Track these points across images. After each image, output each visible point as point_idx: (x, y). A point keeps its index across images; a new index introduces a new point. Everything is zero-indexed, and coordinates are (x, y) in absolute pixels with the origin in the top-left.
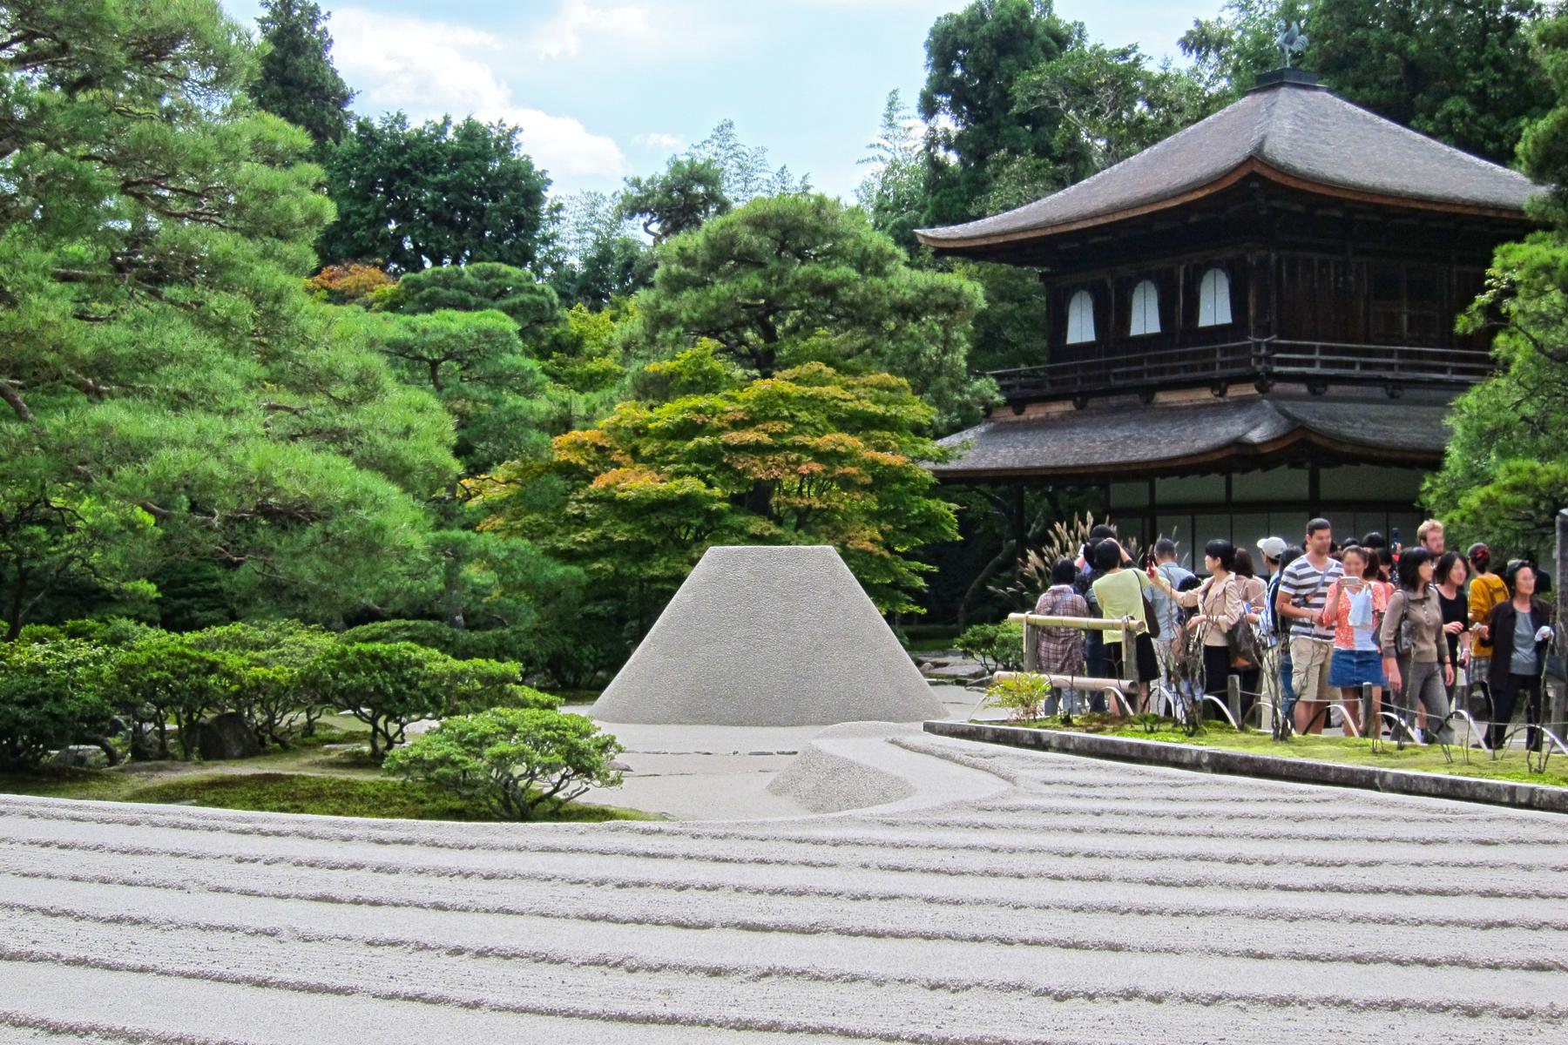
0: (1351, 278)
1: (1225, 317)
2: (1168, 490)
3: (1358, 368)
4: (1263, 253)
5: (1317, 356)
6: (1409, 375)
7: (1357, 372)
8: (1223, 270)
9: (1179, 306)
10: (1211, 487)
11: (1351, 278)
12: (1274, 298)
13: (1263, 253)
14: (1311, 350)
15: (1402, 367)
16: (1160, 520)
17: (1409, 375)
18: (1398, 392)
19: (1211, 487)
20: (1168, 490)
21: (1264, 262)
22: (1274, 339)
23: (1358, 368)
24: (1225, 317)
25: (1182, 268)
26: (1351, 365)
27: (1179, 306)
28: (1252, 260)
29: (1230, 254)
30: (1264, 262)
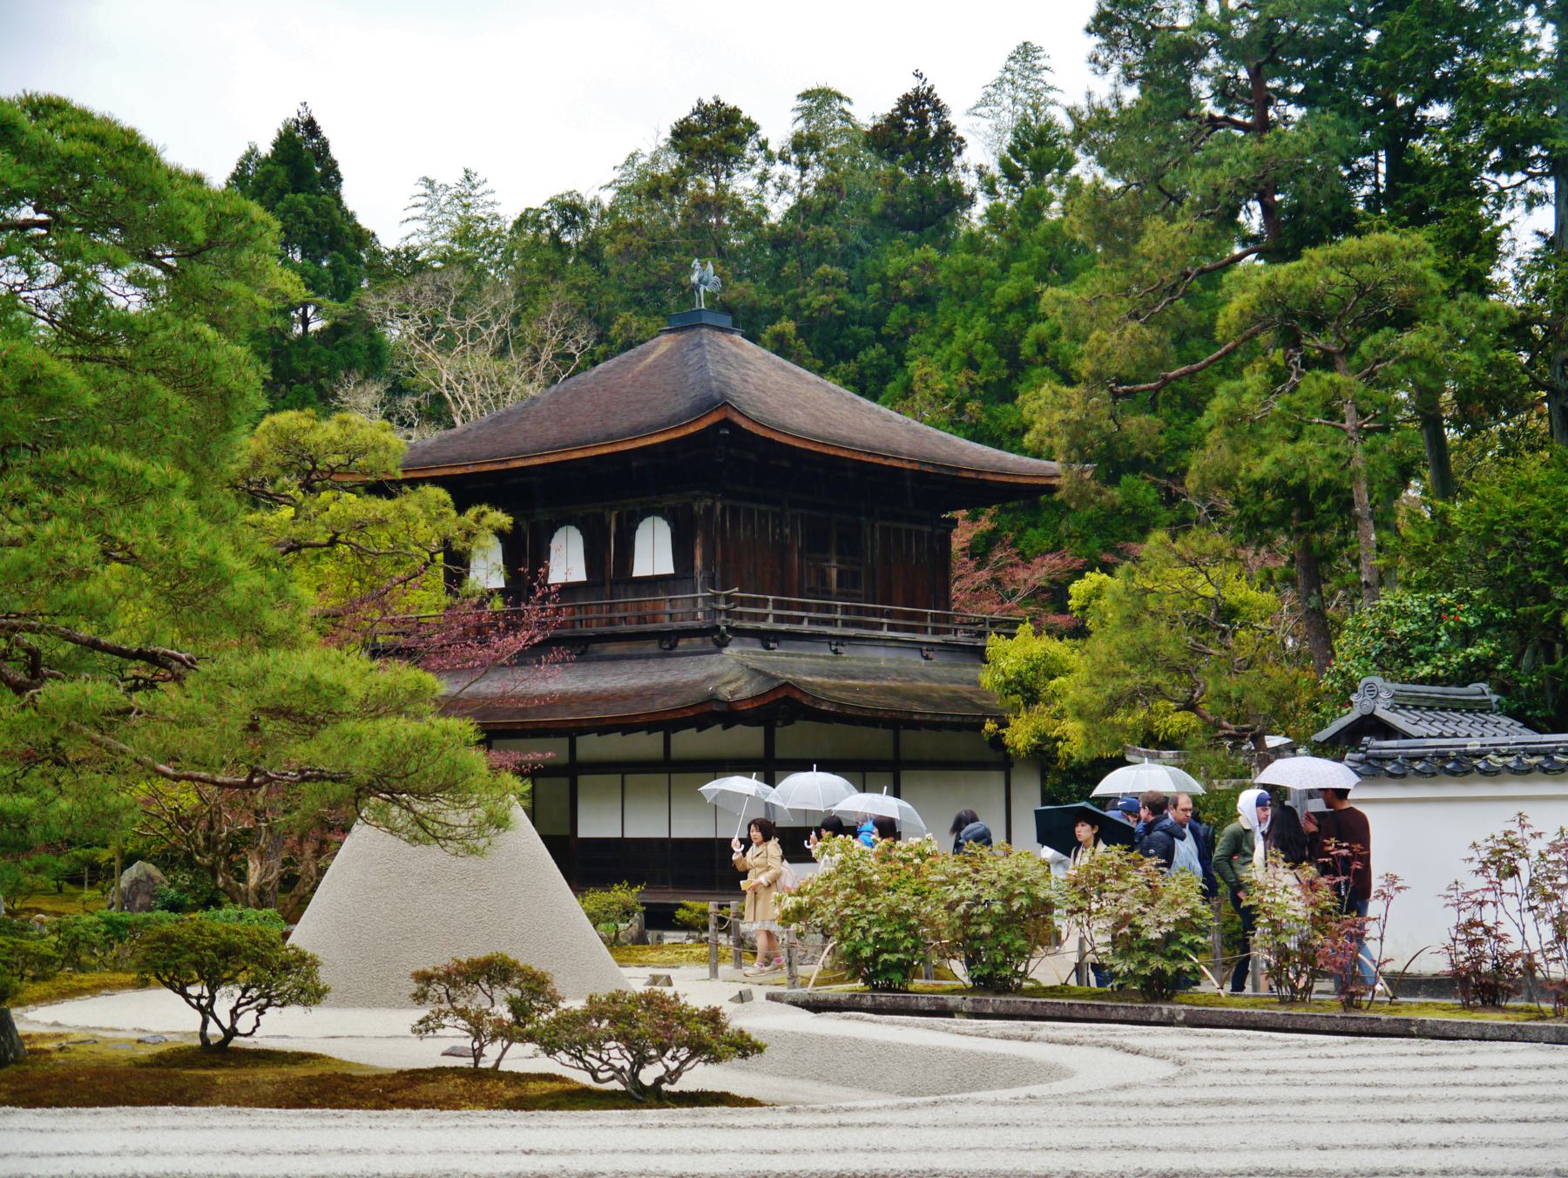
0: (787, 531)
1: (665, 566)
2: (591, 747)
3: (806, 622)
4: (709, 502)
5: (770, 609)
6: (852, 632)
7: (805, 627)
8: (664, 518)
9: (611, 557)
10: (647, 745)
11: (787, 531)
12: (719, 548)
13: (709, 502)
14: (765, 603)
15: (846, 624)
16: (583, 780)
17: (852, 632)
18: (840, 649)
19: (647, 745)
20: (591, 747)
21: (709, 511)
22: (735, 591)
23: (806, 622)
24: (665, 566)
25: (615, 513)
26: (799, 620)
27: (611, 557)
28: (699, 507)
29: (670, 501)
30: (709, 511)
